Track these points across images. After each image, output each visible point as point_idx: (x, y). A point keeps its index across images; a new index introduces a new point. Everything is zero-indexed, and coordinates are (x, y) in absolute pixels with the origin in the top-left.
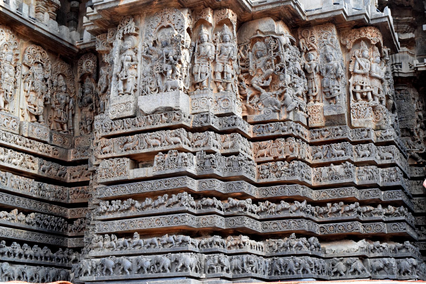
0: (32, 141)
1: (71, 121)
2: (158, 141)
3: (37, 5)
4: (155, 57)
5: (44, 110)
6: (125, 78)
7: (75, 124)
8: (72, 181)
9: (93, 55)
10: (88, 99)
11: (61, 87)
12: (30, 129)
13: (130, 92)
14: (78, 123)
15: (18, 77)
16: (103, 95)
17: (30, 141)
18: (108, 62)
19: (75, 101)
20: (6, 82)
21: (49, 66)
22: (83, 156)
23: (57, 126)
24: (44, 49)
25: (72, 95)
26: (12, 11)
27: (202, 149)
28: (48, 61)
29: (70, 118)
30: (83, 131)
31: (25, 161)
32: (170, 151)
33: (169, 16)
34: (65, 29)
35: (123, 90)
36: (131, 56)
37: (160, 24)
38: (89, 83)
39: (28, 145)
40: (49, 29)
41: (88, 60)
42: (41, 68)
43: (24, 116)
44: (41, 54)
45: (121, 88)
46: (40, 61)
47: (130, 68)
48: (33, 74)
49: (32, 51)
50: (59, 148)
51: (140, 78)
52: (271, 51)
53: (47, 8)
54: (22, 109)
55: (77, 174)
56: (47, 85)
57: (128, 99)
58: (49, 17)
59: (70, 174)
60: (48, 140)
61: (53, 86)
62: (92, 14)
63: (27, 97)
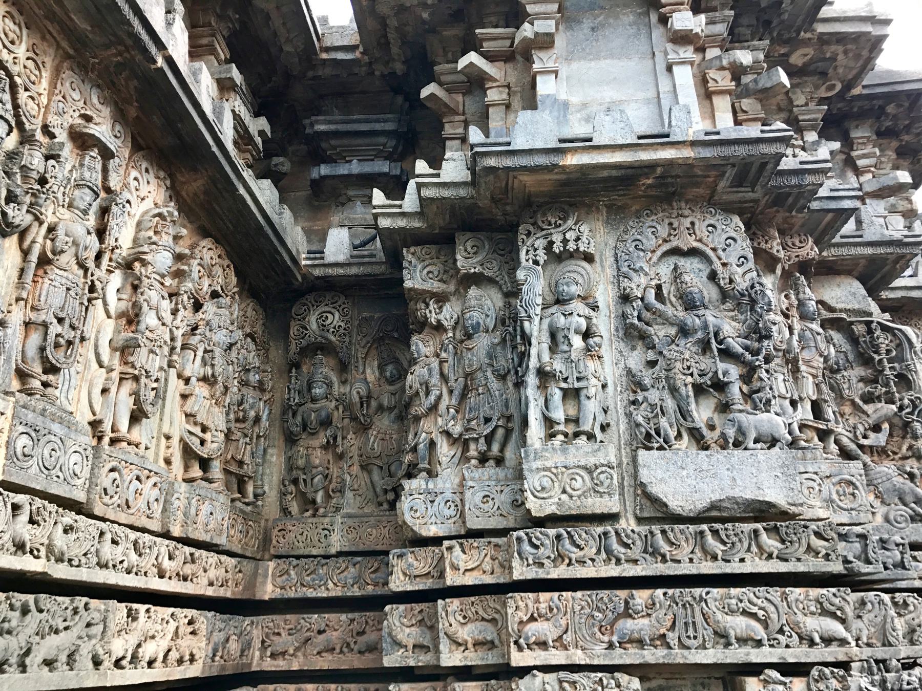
2: (753, 623)
4: (661, 334)
6: (577, 385)
8: (269, 665)
10: (323, 414)
13: (593, 429)
18: (445, 323)
25: (267, 396)
27: (867, 652)
28: (234, 293)
30: (295, 503)
32: (814, 672)
33: (693, 224)
34: (287, 214)
36: (588, 319)
37: (665, 241)
41: (327, 309)
43: (173, 459)
44: (224, 270)
50: (245, 562)
51: (616, 390)
52: (880, 361)
55: (285, 641)
59: (263, 642)
63: (184, 397)
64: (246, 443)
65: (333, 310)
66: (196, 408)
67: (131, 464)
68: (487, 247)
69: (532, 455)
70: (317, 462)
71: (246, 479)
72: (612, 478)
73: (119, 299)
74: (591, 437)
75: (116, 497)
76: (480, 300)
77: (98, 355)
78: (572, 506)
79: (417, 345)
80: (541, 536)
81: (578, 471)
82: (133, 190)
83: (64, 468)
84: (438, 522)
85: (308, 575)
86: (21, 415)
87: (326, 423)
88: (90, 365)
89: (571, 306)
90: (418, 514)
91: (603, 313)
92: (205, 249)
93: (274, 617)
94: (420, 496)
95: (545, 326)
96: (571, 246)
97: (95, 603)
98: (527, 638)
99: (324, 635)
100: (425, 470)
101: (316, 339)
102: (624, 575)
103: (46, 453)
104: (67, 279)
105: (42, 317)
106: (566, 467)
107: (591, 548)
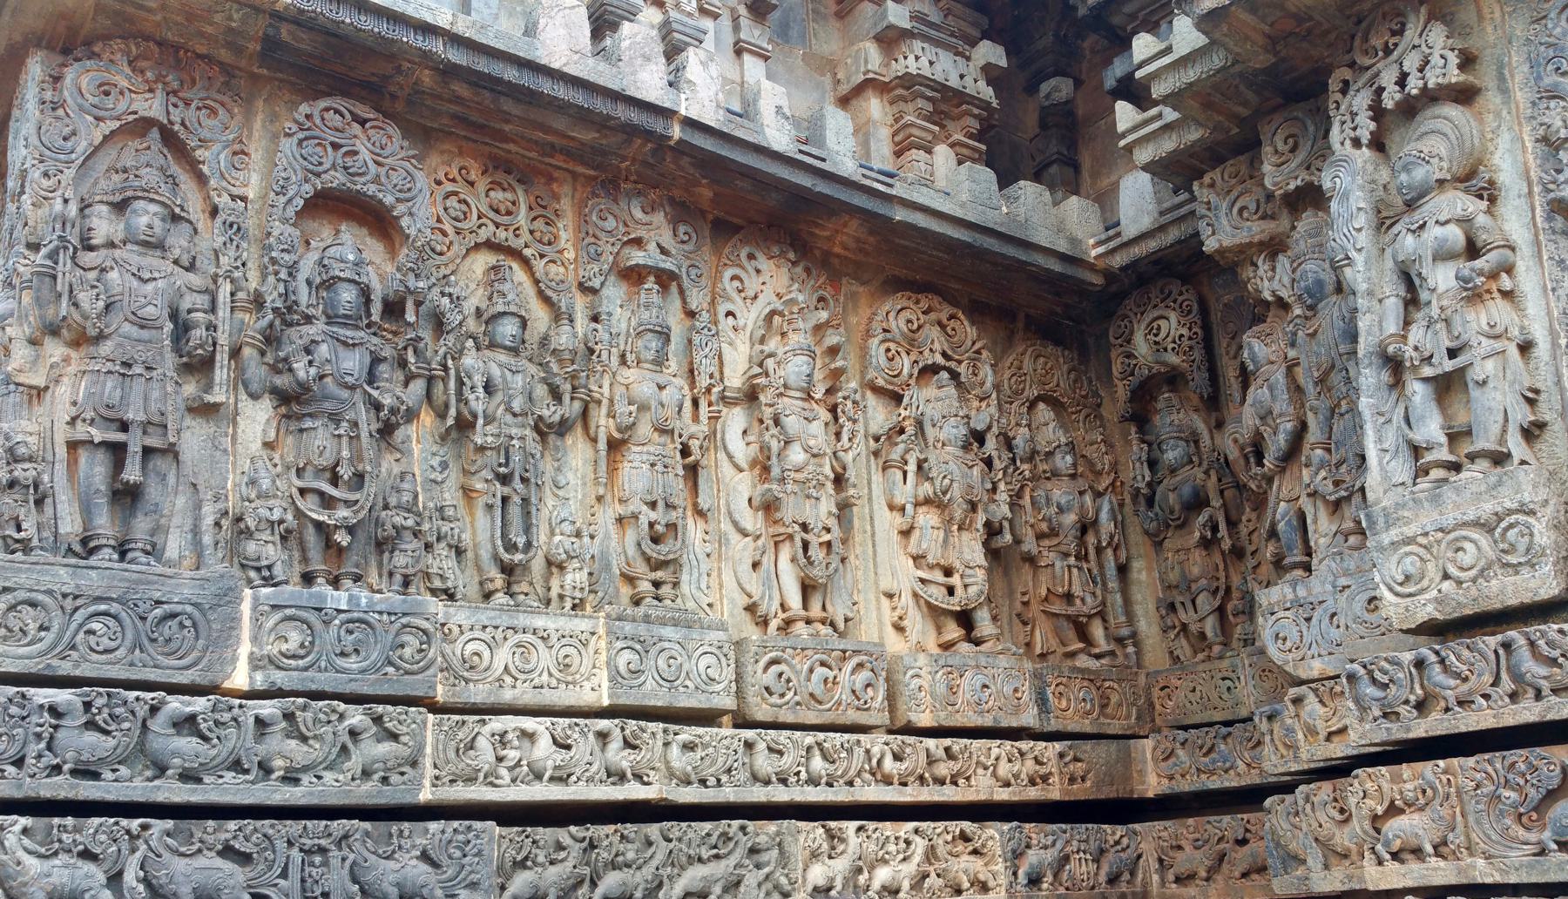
0: (957, 744)
1: (1118, 598)
3: (896, 121)
5: (990, 580)
6: (1449, 366)
7: (1139, 610)
9: (1175, 287)
10: (1187, 490)
11: (1050, 454)
12: (941, 689)
13: (1502, 440)
14: (1152, 606)
15: (850, 455)
16: (1283, 470)
17: (947, 750)
18: (1284, 294)
19: (1121, 505)
20: (796, 488)
21: (987, 372)
22: (1212, 772)
23: (1057, 632)
24: (954, 303)
25: (1105, 482)
26: (776, 147)
28: (978, 352)
29: (1113, 584)
30: (1184, 642)
31: (937, 858)
34: (1028, 192)
35: (1443, 439)
38: (1174, 417)
39: (943, 769)
40: (963, 205)
41: (1156, 313)
42: (951, 391)
43: (905, 623)
45: (1431, 429)
46: (939, 359)
47: (1474, 296)
48: (919, 424)
49: (898, 325)
50: (1088, 746)
51: (1555, 344)
53: (942, 127)
54: (890, 596)
56: (988, 462)
57: (1504, 490)
58: (955, 162)
59: (1161, 861)
60: (1029, 718)
61: (1013, 460)
62: (1166, 60)
63: (906, 533)
64: (1069, 567)
65: (1165, 313)
66: (924, 546)
67: (803, 649)
68: (1311, 129)
69: (1381, 521)
70: (1196, 571)
71: (1084, 620)
72: (1532, 535)
73: (748, 444)
74: (1499, 459)
75: (790, 695)
76: (1318, 235)
77: (735, 524)
78: (1462, 599)
79: (1251, 349)
80: (1387, 666)
81: (1464, 533)
82: (734, 295)
83: (694, 675)
84: (1323, 653)
85: (1205, 755)
86: (615, 629)
87: (1198, 502)
88: (727, 540)
89: (1426, 208)
90: (1289, 644)
91: (1513, 193)
92: (892, 316)
93: (1168, 823)
94: (1287, 614)
95: (1389, 264)
96: (1414, 86)
97: (751, 826)
98: (1387, 844)
99: (1246, 848)
100: (1295, 566)
101: (1150, 369)
102: (1550, 717)
103: (661, 663)
104: (649, 453)
105: (632, 507)
106: (1441, 530)
107: (1480, 675)
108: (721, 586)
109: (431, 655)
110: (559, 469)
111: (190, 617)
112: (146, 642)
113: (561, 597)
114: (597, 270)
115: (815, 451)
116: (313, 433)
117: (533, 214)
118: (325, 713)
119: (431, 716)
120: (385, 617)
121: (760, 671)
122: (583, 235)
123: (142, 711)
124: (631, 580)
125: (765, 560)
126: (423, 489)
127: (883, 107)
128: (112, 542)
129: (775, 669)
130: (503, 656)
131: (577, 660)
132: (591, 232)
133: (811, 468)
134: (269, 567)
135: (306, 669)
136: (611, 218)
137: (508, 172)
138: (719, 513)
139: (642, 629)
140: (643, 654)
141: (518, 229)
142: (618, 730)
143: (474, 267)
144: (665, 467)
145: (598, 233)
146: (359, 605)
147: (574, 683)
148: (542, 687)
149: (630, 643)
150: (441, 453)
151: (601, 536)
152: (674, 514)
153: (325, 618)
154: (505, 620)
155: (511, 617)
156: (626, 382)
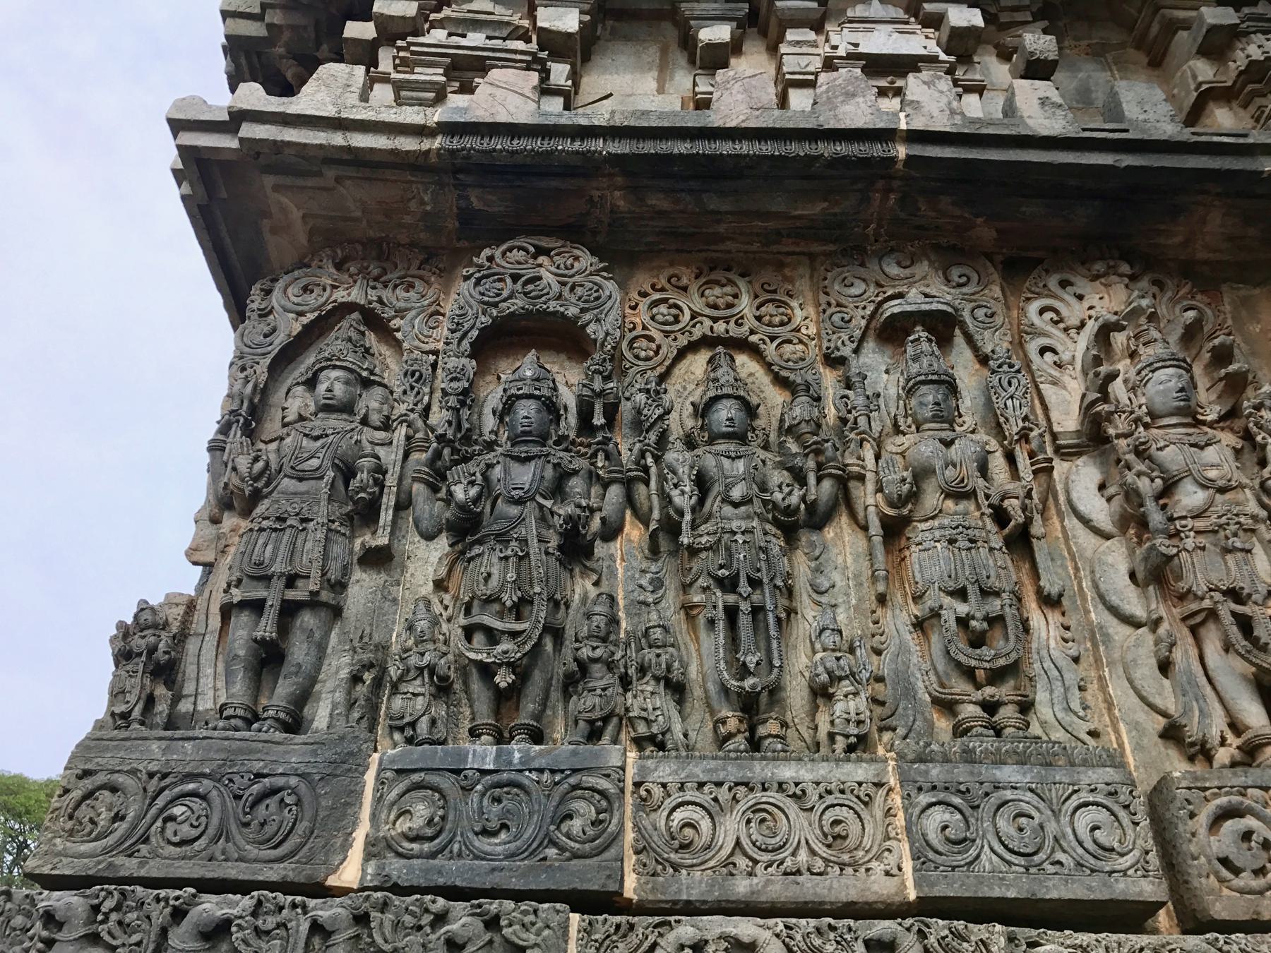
82: (1050, 328)
105: (929, 603)
108: (1110, 705)
109: (612, 828)
110: (818, 570)
111: (294, 791)
112: (234, 828)
113: (832, 737)
114: (845, 338)
115: (1221, 483)
116: (478, 561)
117: (758, 301)
118: (413, 914)
119: (575, 918)
120: (546, 776)
121: (1202, 832)
122: (824, 306)
123: (160, 915)
124: (947, 706)
125: (1178, 655)
126: (628, 614)
127: (1236, 114)
128: (240, 712)
129: (1229, 825)
130: (731, 827)
131: (854, 828)
132: (833, 302)
133: (1219, 509)
134: (413, 725)
135: (433, 855)
136: (857, 282)
137: (728, 269)
138: (1084, 599)
139: (961, 773)
140: (968, 812)
141: (742, 318)
142: (912, 937)
143: (692, 369)
144: (971, 541)
145: (843, 301)
146: (510, 763)
147: (855, 865)
148: (798, 872)
149: (942, 796)
150: (654, 568)
151: (892, 649)
152: (997, 603)
153: (464, 783)
154: (732, 772)
155: (740, 767)
156: (899, 450)
